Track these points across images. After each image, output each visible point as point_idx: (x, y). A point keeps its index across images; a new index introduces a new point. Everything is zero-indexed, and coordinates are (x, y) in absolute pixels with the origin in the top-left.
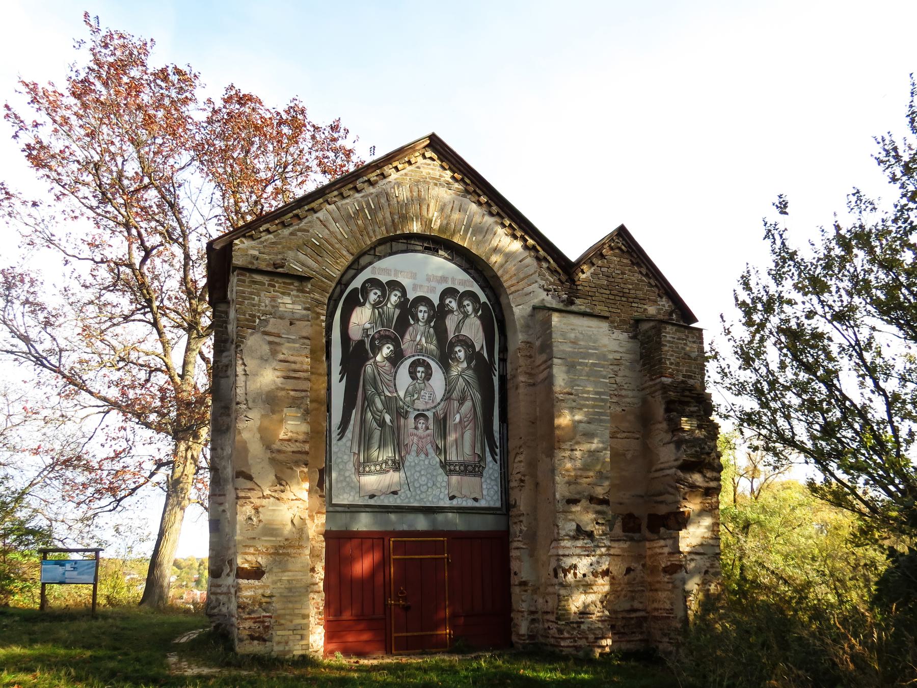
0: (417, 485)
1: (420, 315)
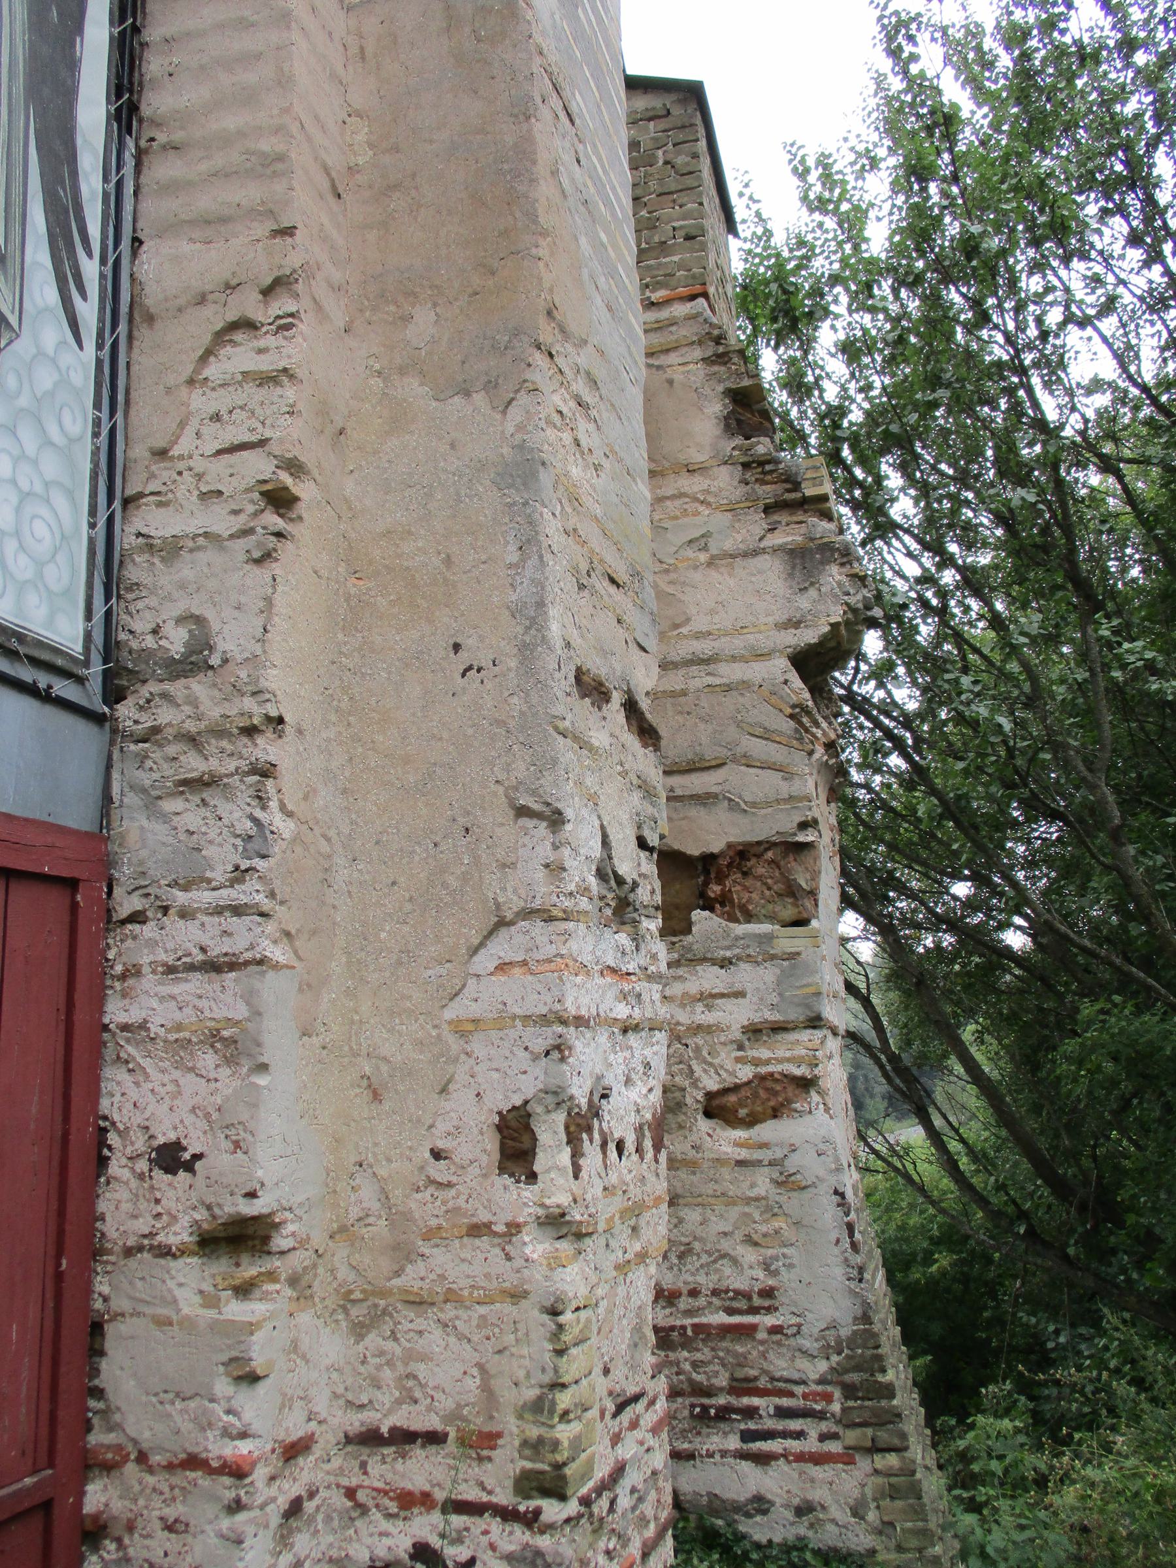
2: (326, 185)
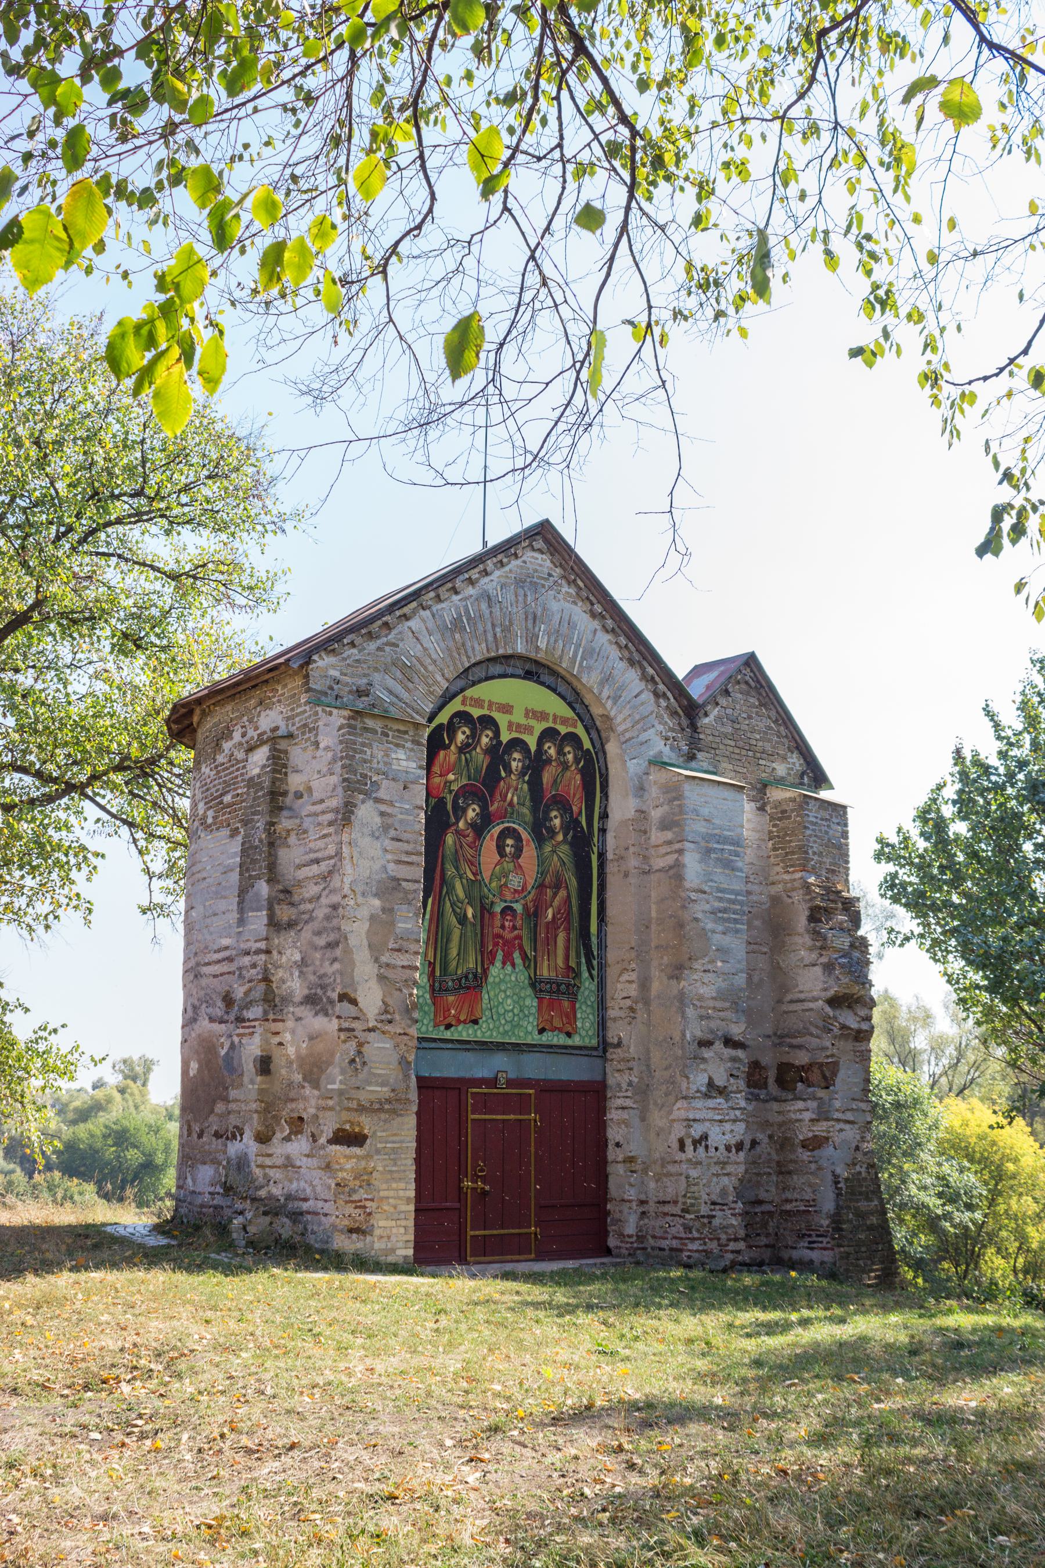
1: (514, 764)
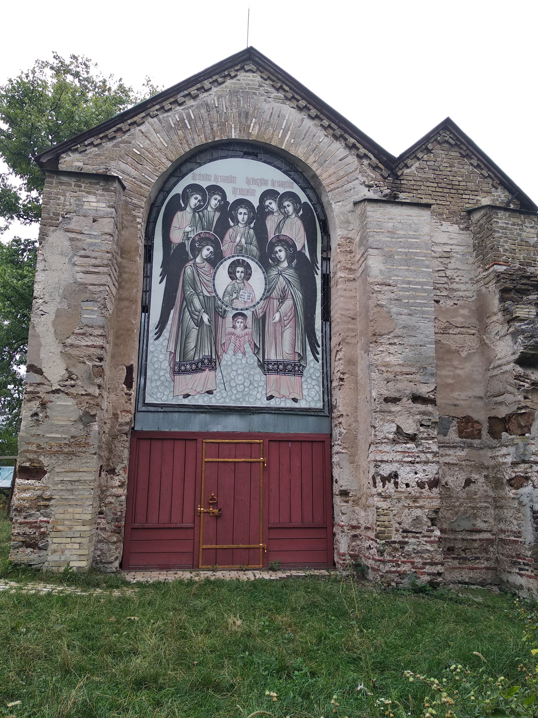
0: (233, 384)
1: (240, 217)
2: (350, 319)
